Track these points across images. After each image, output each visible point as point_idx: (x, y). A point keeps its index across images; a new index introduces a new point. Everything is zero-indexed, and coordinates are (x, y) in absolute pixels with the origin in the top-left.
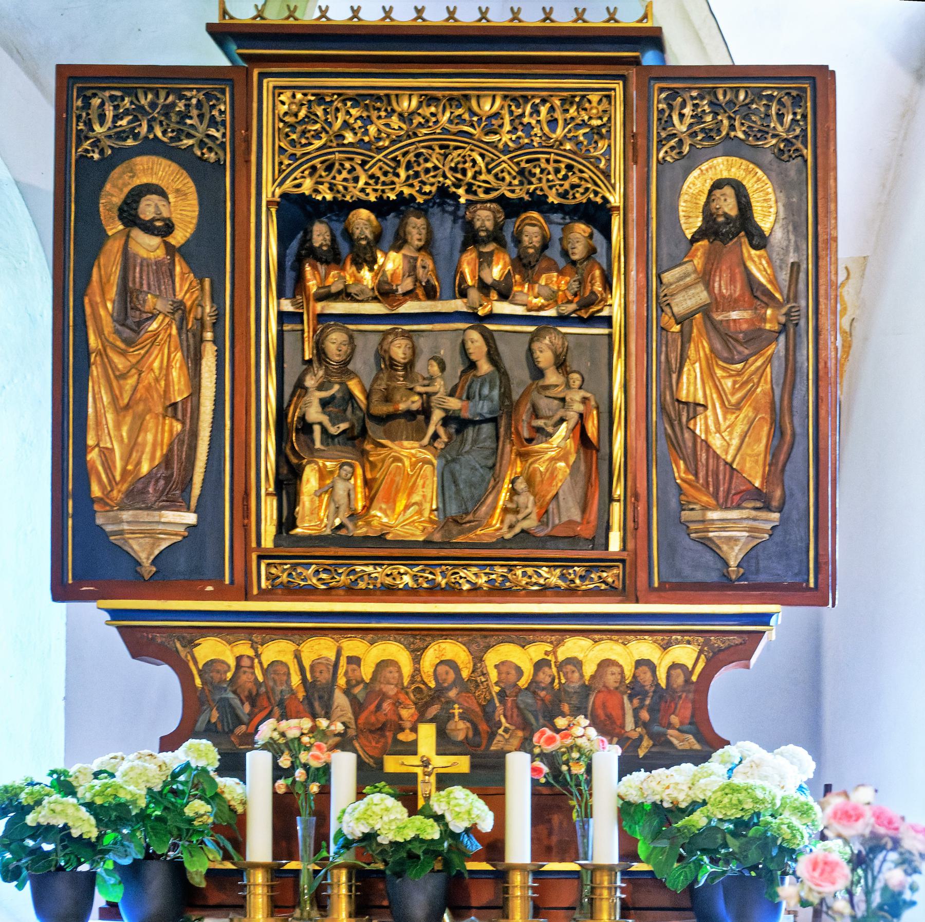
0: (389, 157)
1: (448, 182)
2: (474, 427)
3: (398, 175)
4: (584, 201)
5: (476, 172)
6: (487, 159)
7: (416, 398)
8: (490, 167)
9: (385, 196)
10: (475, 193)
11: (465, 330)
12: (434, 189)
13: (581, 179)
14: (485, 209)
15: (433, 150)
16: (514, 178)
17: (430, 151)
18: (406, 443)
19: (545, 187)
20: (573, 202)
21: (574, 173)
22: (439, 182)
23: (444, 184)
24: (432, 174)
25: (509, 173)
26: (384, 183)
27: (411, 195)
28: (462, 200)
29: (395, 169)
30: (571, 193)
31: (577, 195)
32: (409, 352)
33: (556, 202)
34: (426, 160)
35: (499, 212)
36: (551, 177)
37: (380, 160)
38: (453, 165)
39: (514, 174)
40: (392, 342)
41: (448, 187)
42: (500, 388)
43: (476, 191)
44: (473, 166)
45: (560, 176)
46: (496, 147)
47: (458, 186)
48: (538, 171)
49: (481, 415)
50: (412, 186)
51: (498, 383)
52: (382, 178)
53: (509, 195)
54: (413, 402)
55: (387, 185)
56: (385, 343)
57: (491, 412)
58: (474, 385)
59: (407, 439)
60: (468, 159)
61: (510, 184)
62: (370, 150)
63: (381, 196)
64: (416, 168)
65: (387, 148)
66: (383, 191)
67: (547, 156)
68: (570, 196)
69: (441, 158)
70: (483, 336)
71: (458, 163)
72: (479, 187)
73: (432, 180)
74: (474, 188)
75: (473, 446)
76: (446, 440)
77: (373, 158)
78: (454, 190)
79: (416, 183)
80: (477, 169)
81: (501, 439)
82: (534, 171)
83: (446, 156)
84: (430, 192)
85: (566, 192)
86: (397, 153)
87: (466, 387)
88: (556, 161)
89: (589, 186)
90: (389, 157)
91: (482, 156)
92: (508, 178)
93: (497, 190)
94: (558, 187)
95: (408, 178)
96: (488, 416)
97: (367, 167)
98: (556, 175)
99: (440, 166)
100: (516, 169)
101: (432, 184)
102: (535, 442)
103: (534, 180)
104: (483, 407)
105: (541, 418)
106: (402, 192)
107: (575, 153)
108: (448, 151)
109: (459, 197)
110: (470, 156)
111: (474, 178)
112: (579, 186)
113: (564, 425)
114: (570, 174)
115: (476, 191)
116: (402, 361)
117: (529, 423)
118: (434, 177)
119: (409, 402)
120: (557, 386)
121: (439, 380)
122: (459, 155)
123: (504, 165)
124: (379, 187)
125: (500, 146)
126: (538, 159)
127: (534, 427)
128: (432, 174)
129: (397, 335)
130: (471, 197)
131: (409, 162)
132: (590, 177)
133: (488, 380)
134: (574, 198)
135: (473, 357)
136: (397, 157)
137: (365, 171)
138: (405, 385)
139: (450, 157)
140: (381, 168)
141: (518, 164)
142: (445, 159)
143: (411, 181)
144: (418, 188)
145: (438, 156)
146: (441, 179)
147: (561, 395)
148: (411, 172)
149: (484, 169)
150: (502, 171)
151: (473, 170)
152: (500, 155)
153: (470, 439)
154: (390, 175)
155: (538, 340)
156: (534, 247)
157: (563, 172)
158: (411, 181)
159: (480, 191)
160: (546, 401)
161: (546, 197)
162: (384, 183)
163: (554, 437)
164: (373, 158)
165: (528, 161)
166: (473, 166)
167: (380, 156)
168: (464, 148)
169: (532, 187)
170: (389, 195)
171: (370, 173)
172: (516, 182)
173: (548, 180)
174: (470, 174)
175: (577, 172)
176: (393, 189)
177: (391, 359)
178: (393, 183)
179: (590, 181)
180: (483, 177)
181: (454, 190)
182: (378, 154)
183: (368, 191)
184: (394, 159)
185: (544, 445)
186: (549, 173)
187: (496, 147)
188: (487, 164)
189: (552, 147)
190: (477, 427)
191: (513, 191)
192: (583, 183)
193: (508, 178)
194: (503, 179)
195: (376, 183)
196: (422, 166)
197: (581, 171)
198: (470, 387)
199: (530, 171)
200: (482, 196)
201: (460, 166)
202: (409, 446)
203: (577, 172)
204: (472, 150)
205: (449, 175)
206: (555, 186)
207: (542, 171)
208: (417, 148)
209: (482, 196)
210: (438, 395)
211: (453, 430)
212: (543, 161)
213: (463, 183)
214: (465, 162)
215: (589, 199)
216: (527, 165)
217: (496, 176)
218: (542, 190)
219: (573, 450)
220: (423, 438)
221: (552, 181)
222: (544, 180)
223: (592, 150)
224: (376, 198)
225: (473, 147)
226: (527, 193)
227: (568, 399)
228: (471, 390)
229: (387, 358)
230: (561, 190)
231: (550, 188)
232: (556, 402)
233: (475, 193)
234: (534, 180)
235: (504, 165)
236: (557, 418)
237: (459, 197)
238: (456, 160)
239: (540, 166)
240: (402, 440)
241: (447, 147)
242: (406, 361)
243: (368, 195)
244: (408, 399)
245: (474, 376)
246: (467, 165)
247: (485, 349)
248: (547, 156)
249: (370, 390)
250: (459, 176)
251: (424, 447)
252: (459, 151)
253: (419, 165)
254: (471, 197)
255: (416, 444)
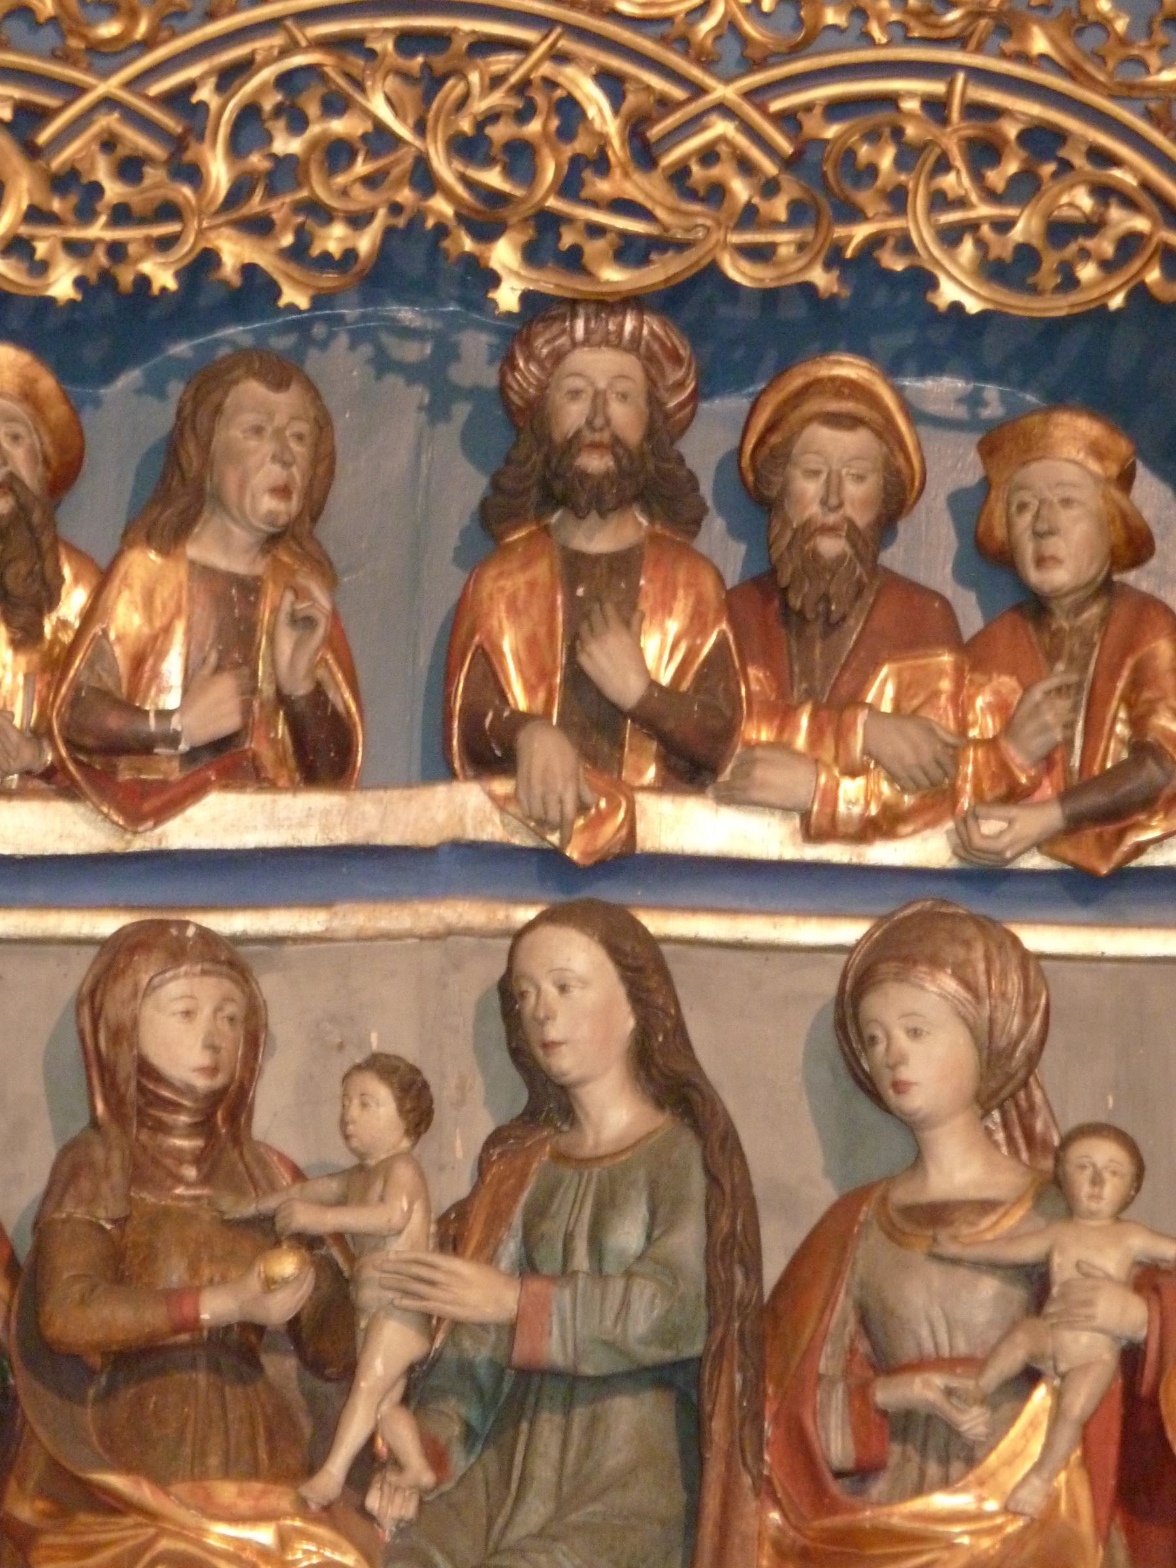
0: (156, 88)
1: (441, 206)
2: (567, 1409)
3: (194, 175)
4: (1117, 302)
5: (577, 163)
6: (632, 100)
7: (287, 1265)
8: (655, 132)
9: (126, 277)
10: (574, 261)
11: (519, 935)
12: (366, 243)
13: (1104, 192)
14: (614, 342)
15: (372, 54)
16: (770, 188)
17: (357, 63)
18: (227, 1492)
19: (922, 232)
20: (1058, 306)
21: (1066, 166)
22: (396, 209)
23: (419, 216)
24: (361, 167)
25: (746, 166)
26: (121, 215)
27: (249, 270)
28: (507, 297)
29: (178, 144)
30: (1051, 260)
31: (1087, 272)
32: (231, 1040)
33: (973, 306)
34: (335, 105)
35: (677, 359)
36: (948, 182)
37: (108, 103)
38: (466, 125)
39: (769, 167)
40: (151, 988)
41: (442, 230)
42: (711, 1222)
43: (576, 252)
44: (566, 133)
45: (997, 178)
46: (684, 43)
47: (487, 232)
48: (886, 160)
49: (609, 1345)
50: (261, 227)
51: (697, 1183)
52: (114, 190)
53: (738, 271)
54: (270, 1284)
55: (143, 221)
56: (121, 990)
57: (665, 1333)
58: (562, 1205)
59: (227, 1472)
60: (540, 100)
61: (749, 217)
62: (66, 57)
63: (107, 279)
64: (286, 144)
65: (148, 44)
66: (117, 251)
67: (937, 87)
68: (1047, 275)
69: (410, 95)
70: (615, 952)
71: (493, 117)
72: (595, 230)
73: (362, 197)
74: (568, 239)
75: (562, 1504)
76: (428, 1478)
77: (79, 90)
78: (468, 244)
79: (279, 208)
80: (581, 145)
81: (715, 1471)
82: (864, 151)
83: (432, 82)
84: (350, 254)
85: (1027, 255)
86: (193, 72)
87: (517, 1219)
88: (974, 110)
89: (1141, 224)
90: (156, 88)
91: (612, 83)
92: (741, 190)
93: (681, 246)
94: (985, 229)
95: (239, 192)
96: (654, 1354)
97: (43, 137)
98: (978, 177)
99: (403, 131)
100: (786, 147)
101: (358, 221)
102: (879, 1487)
103: (864, 197)
104: (625, 1304)
105: (920, 1365)
106: (208, 259)
107: (1073, 72)
108: (440, 63)
109: (494, 280)
110: (550, 84)
111: (569, 187)
112: (1093, 226)
113: (1041, 1396)
114: (1048, 169)
115: (576, 252)
116: (202, 1083)
117: (860, 1394)
118: (370, 181)
119: (254, 1283)
120: (986, 1206)
121: (404, 1174)
122: (496, 81)
123: (721, 127)
124: (97, 230)
125: (706, 26)
126: (890, 100)
127: (884, 1413)
128: (361, 167)
129: (177, 954)
130: (548, 282)
131: (250, 112)
132: (1146, 186)
133: (641, 1175)
134: (1070, 282)
135: (565, 1063)
136: (191, 87)
137: (32, 152)
138: (211, 1201)
139: (453, 89)
140: (109, 143)
141: (789, 120)
142: (427, 98)
143: (255, 204)
144: (287, 240)
145: (392, 83)
146: (406, 195)
147: (1028, 1251)
148: (256, 160)
149: (617, 149)
150: (708, 156)
151: (568, 151)
152: (708, 81)
153: (544, 1471)
154: (153, 175)
155: (900, 978)
156: (853, 533)
157: (1012, 167)
158: (255, 204)
159: (594, 248)
160: (936, 1274)
161: (924, 280)
162: (121, 215)
163: (993, 1459)
164: (79, 90)
165: (836, 109)
166: (566, 133)
167: (111, 86)
168: (524, 48)
169: (860, 232)
170: (147, 267)
171: (57, 162)
172: (779, 208)
173: (940, 201)
174: (549, 172)
175: (1079, 161)
176: (165, 244)
177: (146, 1069)
178: (169, 211)
179: (1143, 199)
180: (603, 187)
181: (468, 244)
182: (105, 75)
183: (41, 249)
184: (179, 99)
185: (940, 1501)
186: (943, 165)
187: (684, 43)
188: (636, 129)
189: (960, 41)
190: (580, 1415)
191: (760, 254)
192: (1115, 213)
193: (741, 190)
194: (717, 193)
195: (85, 214)
196: (315, 129)
197: (1101, 157)
198: (537, 1213)
199: (850, 154)
200: (613, 275)
201: (499, 132)
202: (244, 1506)
203: (1079, 161)
204: (561, 58)
205: (444, 168)
206: (972, 226)
207: (908, 156)
208: (291, 48)
209: (613, 275)
210: (398, 1247)
211: (456, 1429)
212: (911, 105)
213: (513, 216)
214: (523, 115)
215: (1139, 293)
216: (831, 131)
217: (679, 176)
218: (905, 245)
219: (1086, 1526)
220: (312, 1467)
221: (962, 203)
222: (920, 202)
223: (1154, 60)
224: (79, 283)
225: (565, 44)
226: (834, 259)
227: (1063, 1269)
228: (553, 1228)
229: (126, 1067)
230: (1002, 247)
231: (950, 237)
232: (989, 1287)
233: (574, 261)
234: (864, 197)
235: (721, 127)
236: (1009, 1361)
237: (494, 280)
238: (480, 105)
239: (898, 133)
240: (204, 1475)
241: (438, 40)
242: (220, 1080)
243: (41, 268)
244: (249, 1265)
245: (561, 1157)
246: (534, 127)
247: (628, 1023)
248: (937, 87)
249: (42, 1227)
250: (493, 178)
251: (328, 1514)
252: (500, 62)
253: (298, 123)
254: (548, 282)
255: (281, 1498)
